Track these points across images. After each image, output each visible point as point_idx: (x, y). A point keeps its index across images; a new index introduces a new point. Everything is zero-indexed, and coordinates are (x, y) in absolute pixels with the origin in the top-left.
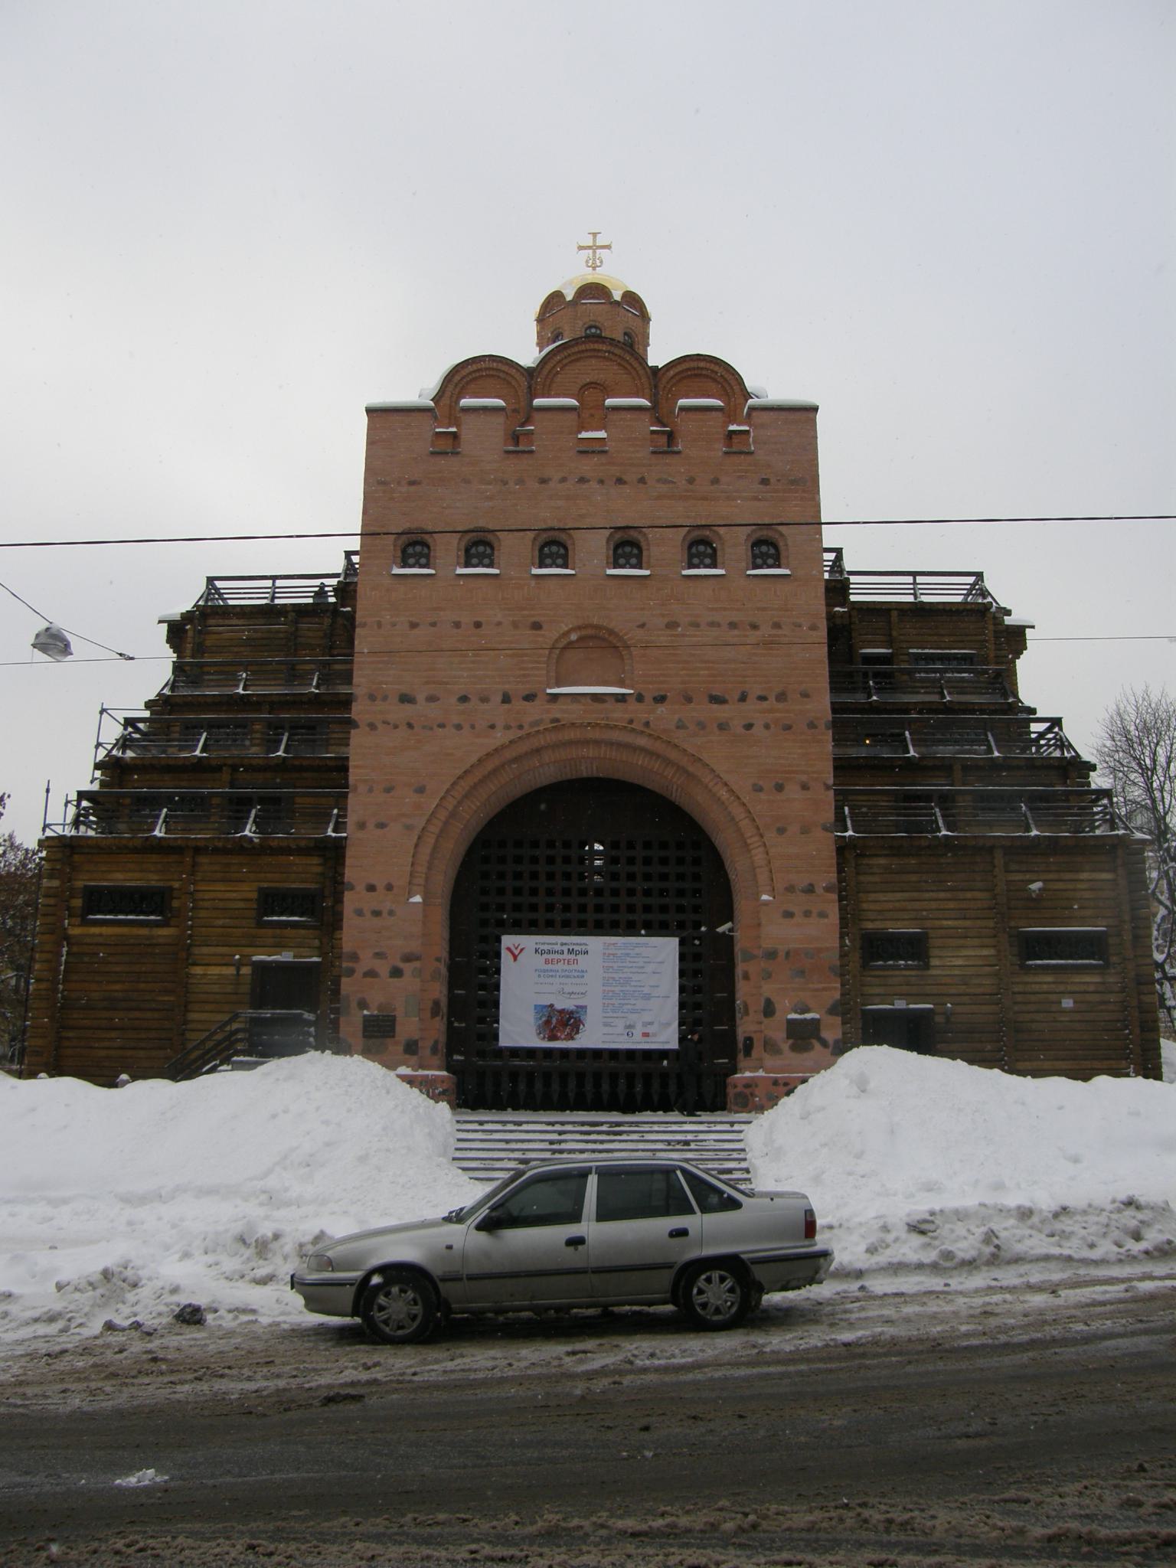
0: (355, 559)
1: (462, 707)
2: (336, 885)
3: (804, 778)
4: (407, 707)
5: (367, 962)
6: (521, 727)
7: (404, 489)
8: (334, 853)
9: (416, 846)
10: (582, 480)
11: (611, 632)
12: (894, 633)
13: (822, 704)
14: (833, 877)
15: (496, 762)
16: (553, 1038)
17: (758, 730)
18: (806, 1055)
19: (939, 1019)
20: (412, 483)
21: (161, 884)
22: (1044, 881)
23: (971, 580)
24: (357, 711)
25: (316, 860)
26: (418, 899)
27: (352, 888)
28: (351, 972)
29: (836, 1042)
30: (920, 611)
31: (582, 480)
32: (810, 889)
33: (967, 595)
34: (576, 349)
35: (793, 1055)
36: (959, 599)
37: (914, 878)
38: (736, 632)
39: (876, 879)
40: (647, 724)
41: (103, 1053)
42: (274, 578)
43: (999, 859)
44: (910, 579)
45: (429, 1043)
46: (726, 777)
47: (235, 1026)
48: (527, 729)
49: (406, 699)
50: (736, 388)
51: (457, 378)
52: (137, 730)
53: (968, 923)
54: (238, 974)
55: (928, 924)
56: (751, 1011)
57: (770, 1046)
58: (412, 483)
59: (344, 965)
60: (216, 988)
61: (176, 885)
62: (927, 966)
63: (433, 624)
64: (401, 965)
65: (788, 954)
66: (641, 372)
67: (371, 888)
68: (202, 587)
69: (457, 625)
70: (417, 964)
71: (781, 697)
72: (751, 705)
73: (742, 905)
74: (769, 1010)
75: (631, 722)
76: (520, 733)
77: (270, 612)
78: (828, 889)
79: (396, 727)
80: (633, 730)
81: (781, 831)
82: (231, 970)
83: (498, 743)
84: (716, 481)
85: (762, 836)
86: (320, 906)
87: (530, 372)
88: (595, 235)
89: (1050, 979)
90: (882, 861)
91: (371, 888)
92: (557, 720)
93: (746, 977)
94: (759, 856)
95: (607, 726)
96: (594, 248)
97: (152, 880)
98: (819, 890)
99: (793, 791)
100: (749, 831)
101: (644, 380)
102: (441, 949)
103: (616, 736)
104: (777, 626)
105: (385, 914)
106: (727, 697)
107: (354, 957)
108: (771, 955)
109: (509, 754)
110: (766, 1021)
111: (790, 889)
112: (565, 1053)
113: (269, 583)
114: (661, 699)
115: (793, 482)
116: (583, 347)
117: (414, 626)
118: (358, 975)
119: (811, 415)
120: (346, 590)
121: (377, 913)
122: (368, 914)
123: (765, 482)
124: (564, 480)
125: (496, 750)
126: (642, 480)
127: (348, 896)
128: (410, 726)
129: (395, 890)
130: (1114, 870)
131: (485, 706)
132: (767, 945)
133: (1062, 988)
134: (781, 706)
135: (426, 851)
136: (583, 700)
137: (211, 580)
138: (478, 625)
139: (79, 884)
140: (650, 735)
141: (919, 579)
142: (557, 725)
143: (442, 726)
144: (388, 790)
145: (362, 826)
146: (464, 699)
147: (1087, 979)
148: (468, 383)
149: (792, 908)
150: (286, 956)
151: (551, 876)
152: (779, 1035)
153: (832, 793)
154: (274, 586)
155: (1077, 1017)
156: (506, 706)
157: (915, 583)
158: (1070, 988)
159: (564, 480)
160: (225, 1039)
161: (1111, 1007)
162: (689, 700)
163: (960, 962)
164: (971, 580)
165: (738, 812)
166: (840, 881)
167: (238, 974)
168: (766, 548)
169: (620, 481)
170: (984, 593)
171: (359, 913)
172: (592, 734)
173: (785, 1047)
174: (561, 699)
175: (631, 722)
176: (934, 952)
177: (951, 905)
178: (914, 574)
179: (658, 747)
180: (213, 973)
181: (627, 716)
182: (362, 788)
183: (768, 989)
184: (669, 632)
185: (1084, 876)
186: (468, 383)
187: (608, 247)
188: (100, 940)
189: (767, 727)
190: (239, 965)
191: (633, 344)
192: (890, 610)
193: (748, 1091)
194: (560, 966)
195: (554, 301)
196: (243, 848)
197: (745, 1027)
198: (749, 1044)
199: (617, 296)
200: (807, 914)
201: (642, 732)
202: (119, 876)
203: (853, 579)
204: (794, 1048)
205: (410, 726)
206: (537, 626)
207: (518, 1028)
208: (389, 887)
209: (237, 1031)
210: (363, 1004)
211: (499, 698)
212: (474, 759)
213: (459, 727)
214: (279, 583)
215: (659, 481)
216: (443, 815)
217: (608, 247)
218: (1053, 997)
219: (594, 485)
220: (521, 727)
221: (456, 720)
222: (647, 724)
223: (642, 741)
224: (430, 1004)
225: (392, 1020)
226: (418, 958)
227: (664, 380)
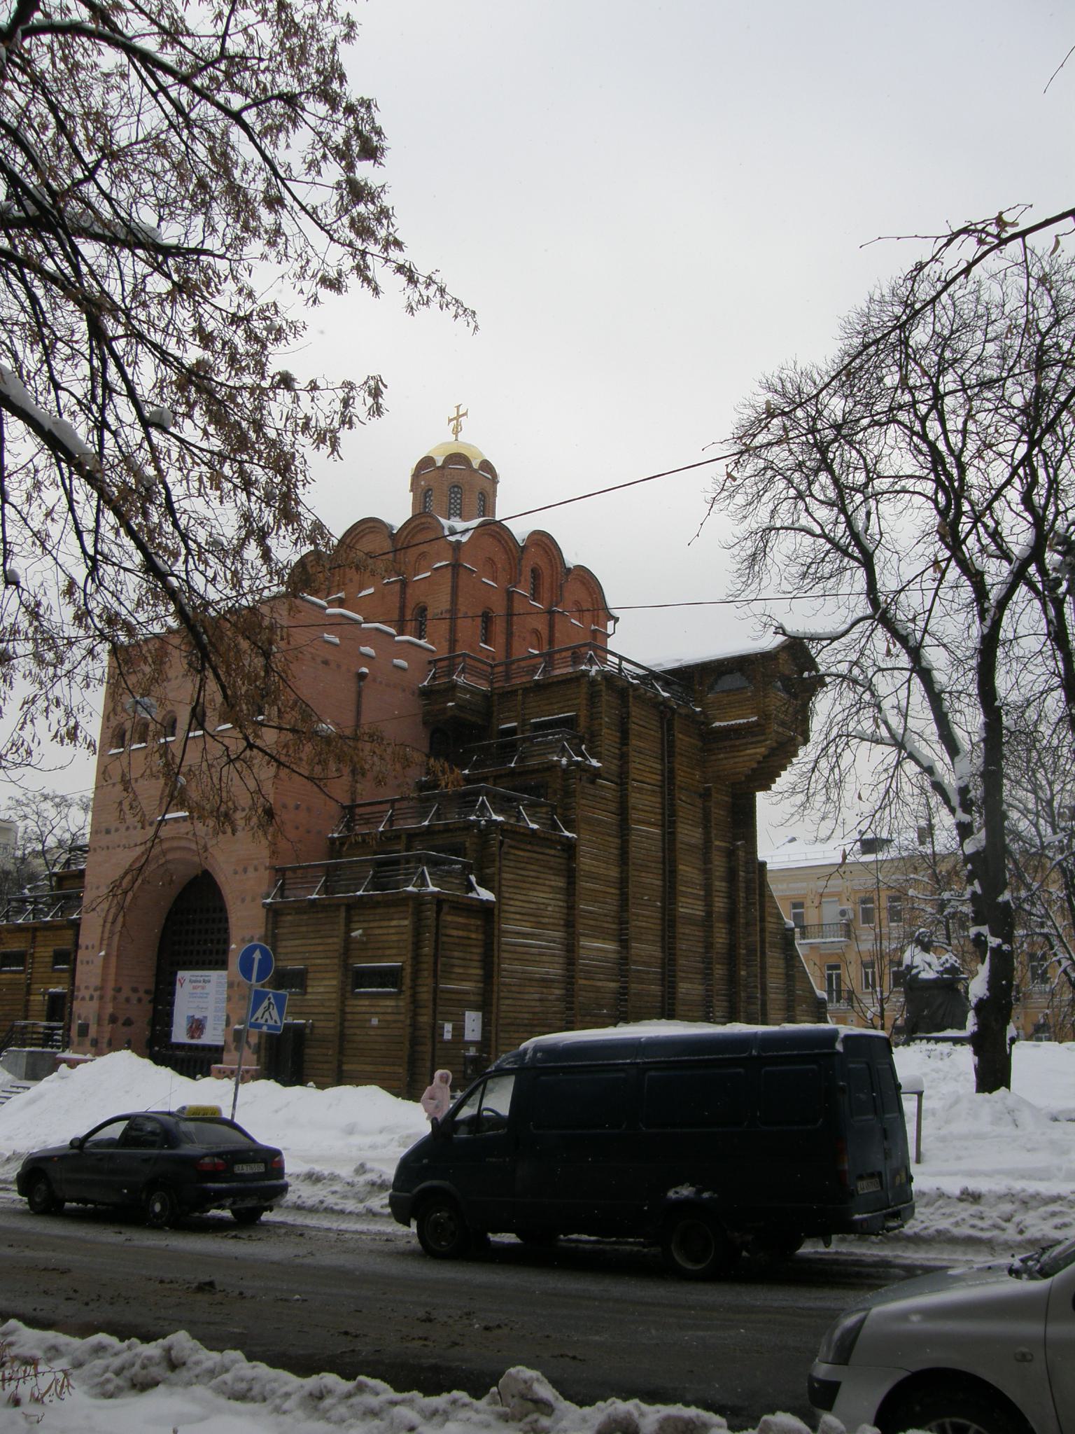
2: (77, 945)
3: (256, 862)
8: (76, 925)
16: (192, 1037)
19: (308, 1031)
22: (364, 929)
26: (103, 953)
37: (304, 929)
39: (285, 930)
45: (106, 1040)
53: (328, 961)
55: (308, 962)
62: (305, 993)
89: (367, 1003)
90: (289, 918)
91: (87, 948)
107: (79, 990)
112: (196, 1047)
133: (373, 1010)
147: (388, 1003)
150: (58, 990)
155: (379, 1032)
161: (400, 1025)
163: (321, 990)
172: (175, 844)
176: (309, 982)
177: (320, 948)
180: (38, 999)
185: (394, 923)
190: (44, 994)
192: (516, 691)
194: (199, 991)
196: (48, 927)
207: (180, 1034)
210: (79, 1018)
218: (367, 1016)
224: (107, 1017)
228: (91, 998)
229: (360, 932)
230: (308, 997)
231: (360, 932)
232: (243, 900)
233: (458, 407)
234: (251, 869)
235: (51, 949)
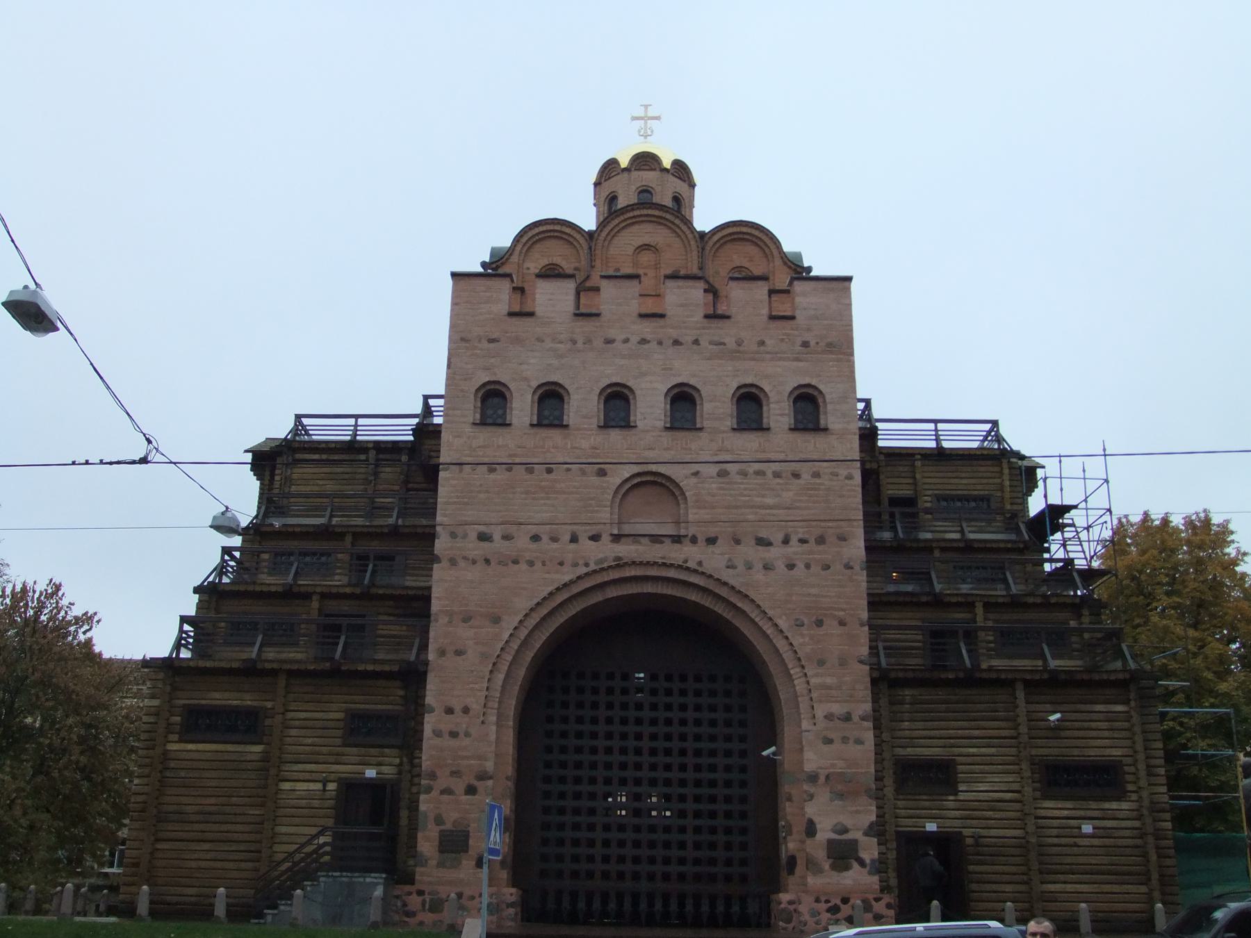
0: (432, 402)
1: (534, 546)
2: (416, 707)
4: (486, 545)
5: (443, 781)
6: (587, 565)
7: (485, 345)
8: (413, 677)
9: (491, 672)
10: (643, 341)
12: (918, 476)
13: (857, 548)
14: (867, 707)
15: (564, 596)
17: (800, 569)
18: (845, 874)
19: (969, 841)
20: (491, 341)
21: (255, 704)
23: (987, 427)
24: (441, 545)
25: (398, 683)
27: (432, 710)
28: (429, 790)
29: (873, 861)
30: (940, 456)
31: (643, 341)
32: (847, 718)
33: (983, 441)
34: (631, 214)
35: (834, 873)
36: (975, 445)
38: (778, 480)
40: (700, 563)
41: (194, 864)
42: (357, 417)
43: (1020, 694)
44: (932, 426)
46: (770, 613)
47: (322, 840)
48: (593, 567)
49: (483, 537)
50: (775, 252)
51: (524, 239)
52: (233, 558)
53: (993, 750)
54: (324, 790)
56: (795, 830)
57: (812, 865)
58: (491, 341)
59: (423, 782)
61: (269, 705)
64: (476, 783)
65: (827, 777)
66: (690, 236)
67: (450, 711)
68: (291, 424)
70: (490, 783)
72: (794, 547)
73: (788, 733)
74: (811, 829)
75: (686, 561)
76: (585, 570)
77: (353, 448)
78: (863, 718)
79: (474, 562)
80: (688, 569)
81: (821, 663)
82: (319, 786)
83: (567, 578)
84: (762, 343)
85: (803, 667)
86: (401, 730)
87: (591, 234)
88: (646, 107)
91: (450, 711)
92: (619, 558)
93: (790, 799)
94: (800, 685)
95: (664, 564)
96: (646, 119)
97: (247, 700)
98: (856, 718)
99: (831, 627)
101: (693, 243)
102: (510, 770)
103: (672, 574)
105: (462, 735)
106: (772, 540)
107: (433, 776)
108: (813, 778)
109: (576, 589)
110: (809, 841)
111: (829, 717)
113: (352, 421)
114: (711, 541)
115: (830, 345)
116: (637, 213)
119: (846, 284)
120: (426, 431)
121: (454, 735)
122: (447, 736)
124: (626, 341)
125: (565, 585)
126: (696, 342)
127: (427, 718)
128: (487, 561)
129: (471, 713)
130: (1126, 702)
131: (555, 546)
132: (808, 767)
133: (1081, 813)
134: (821, 548)
135: (500, 677)
136: (643, 540)
137: (298, 417)
140: (703, 573)
141: (940, 426)
142: (620, 564)
143: (516, 562)
145: (442, 653)
146: (536, 538)
148: (534, 243)
149: (831, 735)
151: (610, 706)
152: (821, 855)
153: (866, 628)
154: (356, 425)
156: (573, 546)
157: (936, 430)
158: (1089, 813)
159: (626, 341)
160: (315, 851)
162: (738, 542)
164: (987, 427)
165: (781, 644)
166: (874, 710)
167: (324, 790)
168: (807, 403)
169: (676, 342)
170: (999, 439)
171: (437, 733)
173: (827, 867)
174: (623, 540)
175: (686, 561)
178: (936, 422)
179: (710, 585)
181: (683, 556)
182: (443, 620)
183: (811, 810)
184: (721, 480)
186: (534, 243)
187: (657, 118)
189: (808, 566)
191: (680, 208)
192: (913, 455)
193: (792, 908)
195: (610, 169)
197: (791, 846)
198: (792, 861)
199: (667, 164)
200: (845, 740)
201: (695, 571)
202: (217, 695)
203: (880, 425)
204: (834, 867)
205: (487, 561)
208: (466, 710)
209: (325, 844)
211: (568, 537)
212: (545, 594)
213: (531, 563)
214: (361, 421)
215: (711, 343)
216: (515, 645)
217: (657, 118)
219: (654, 345)
220: (587, 565)
221: (528, 556)
222: (700, 563)
223: (694, 579)
225: (466, 835)
226: (491, 778)
227: (711, 243)
229: (1058, 716)
230: (962, 796)
231: (1058, 716)
233: (646, 107)
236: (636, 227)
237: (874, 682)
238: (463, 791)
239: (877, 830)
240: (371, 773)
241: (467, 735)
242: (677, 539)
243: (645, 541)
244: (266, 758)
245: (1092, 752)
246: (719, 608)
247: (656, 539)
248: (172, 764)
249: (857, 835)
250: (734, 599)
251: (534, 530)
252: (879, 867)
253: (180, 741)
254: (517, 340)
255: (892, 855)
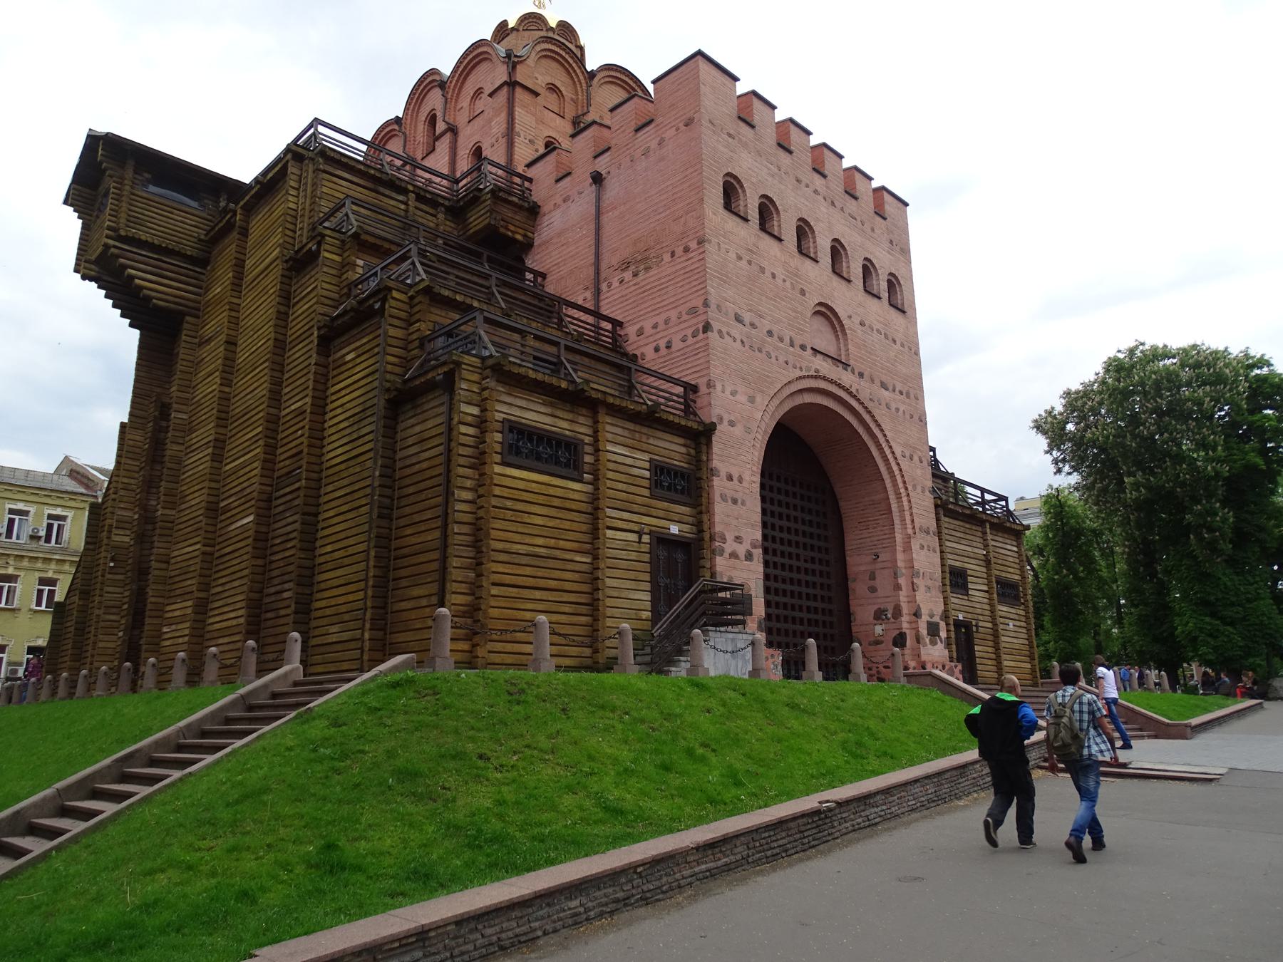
5: (730, 546)
11: (836, 314)
17: (901, 412)
20: (730, 135)
31: (816, 192)
48: (804, 373)
49: (738, 319)
54: (640, 542)
58: (730, 135)
60: (623, 554)
63: (750, 263)
67: (730, 478)
69: (762, 270)
71: (908, 396)
74: (917, 614)
76: (801, 374)
80: (851, 394)
82: (634, 537)
84: (873, 230)
91: (730, 478)
94: (906, 503)
100: (901, 485)
104: (902, 345)
107: (724, 540)
117: (740, 258)
118: (726, 555)
121: (735, 501)
123: (891, 242)
127: (716, 482)
129: (745, 484)
137: (317, 122)
138: (774, 276)
139: (499, 416)
143: (760, 350)
144: (734, 393)
148: (546, 56)
159: (807, 186)
167: (640, 542)
174: (819, 356)
176: (970, 586)
188: (521, 485)
201: (854, 397)
206: (803, 292)
208: (740, 480)
219: (820, 198)
228: (749, 556)
232: (914, 487)
234: (916, 458)
235: (647, 457)
236: (614, 87)
237: (936, 506)
238: (743, 557)
239: (945, 615)
240: (674, 529)
241: (743, 503)
242: (846, 366)
243: (829, 360)
244: (595, 499)
245: (1009, 576)
246: (861, 430)
247: (836, 361)
248: (497, 491)
249: (937, 619)
250: (872, 425)
251: (765, 325)
252: (948, 645)
253: (504, 464)
254: (745, 145)
255: (953, 635)
